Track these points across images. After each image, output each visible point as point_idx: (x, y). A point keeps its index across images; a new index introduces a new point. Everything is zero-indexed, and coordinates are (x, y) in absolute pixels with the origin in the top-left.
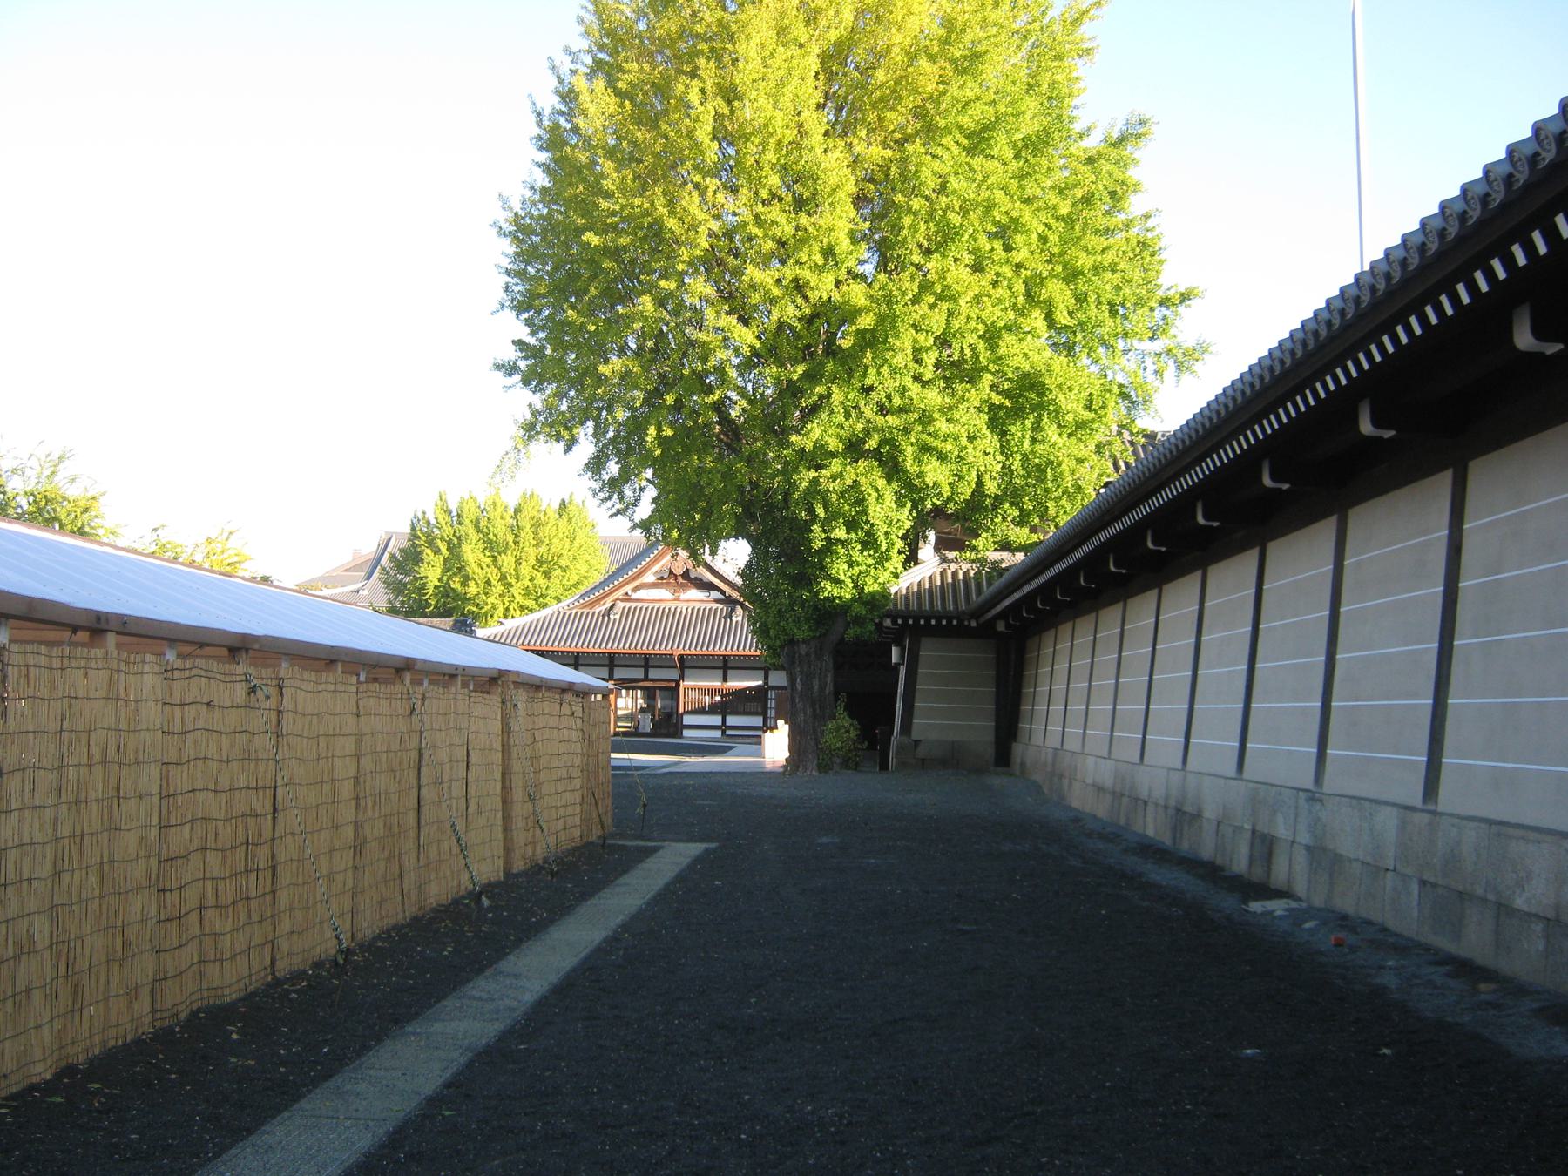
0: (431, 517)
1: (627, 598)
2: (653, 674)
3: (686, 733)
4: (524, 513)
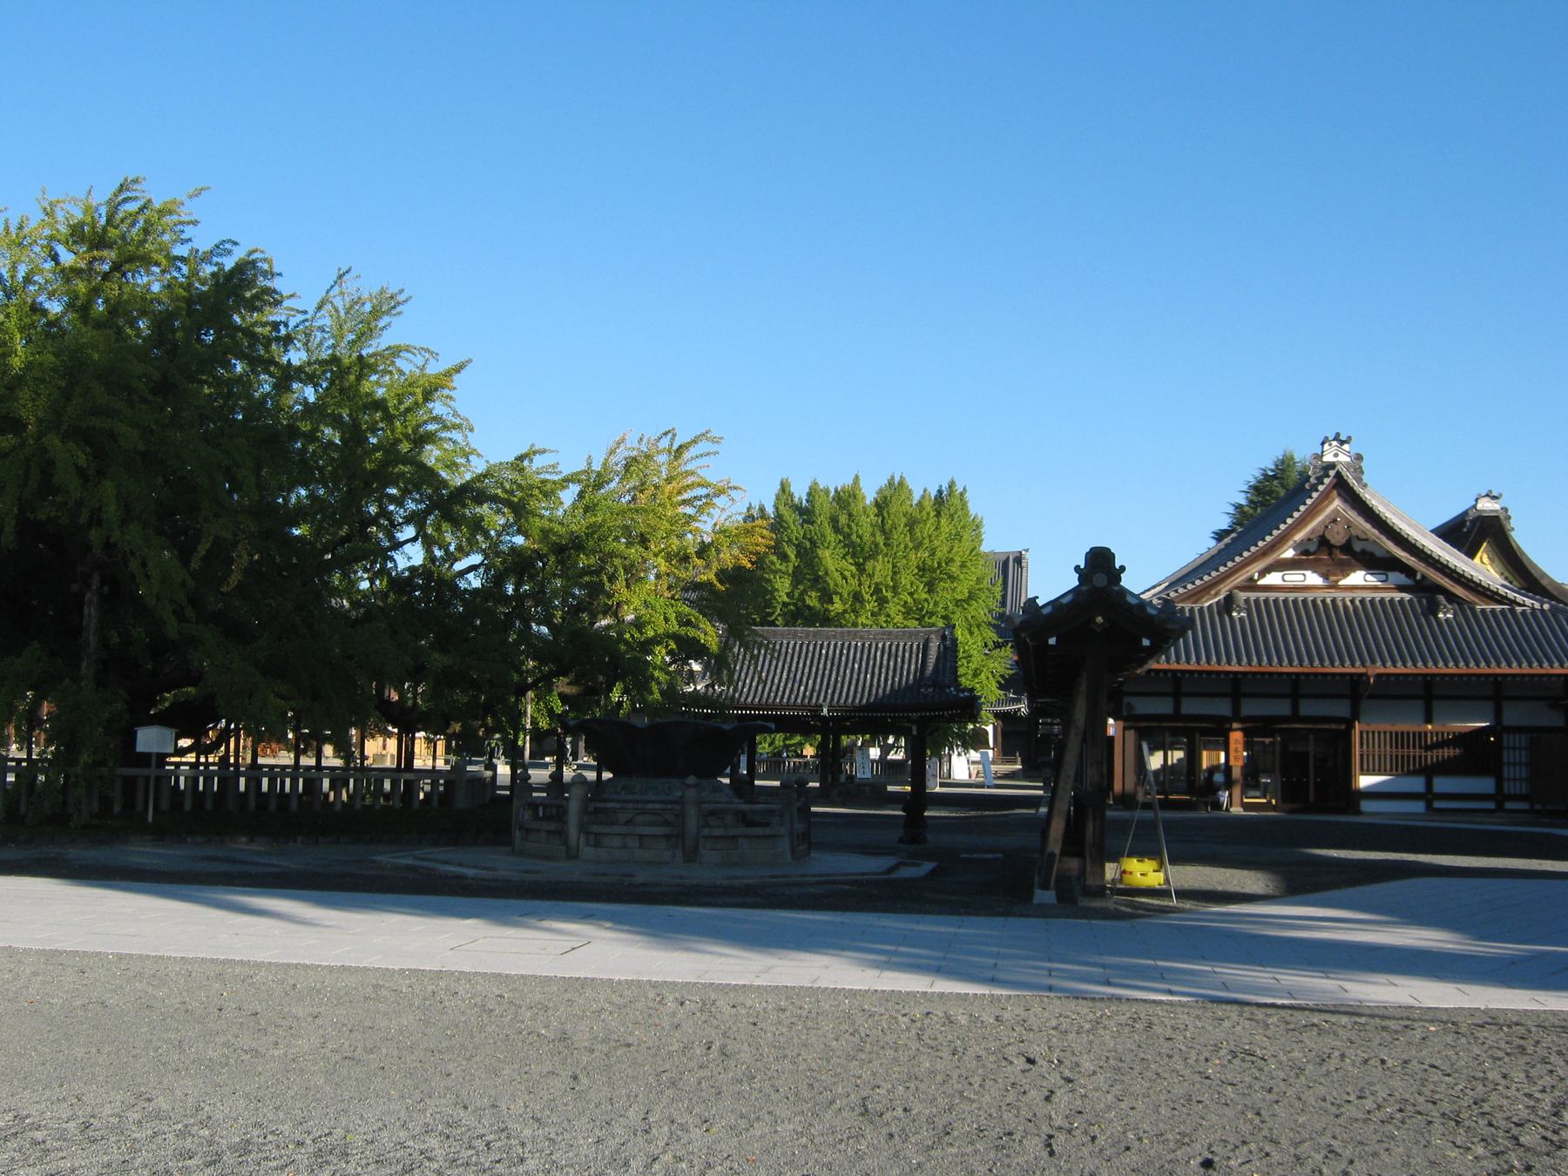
0: (770, 510)
1: (1250, 585)
2: (1308, 708)
3: (1366, 806)
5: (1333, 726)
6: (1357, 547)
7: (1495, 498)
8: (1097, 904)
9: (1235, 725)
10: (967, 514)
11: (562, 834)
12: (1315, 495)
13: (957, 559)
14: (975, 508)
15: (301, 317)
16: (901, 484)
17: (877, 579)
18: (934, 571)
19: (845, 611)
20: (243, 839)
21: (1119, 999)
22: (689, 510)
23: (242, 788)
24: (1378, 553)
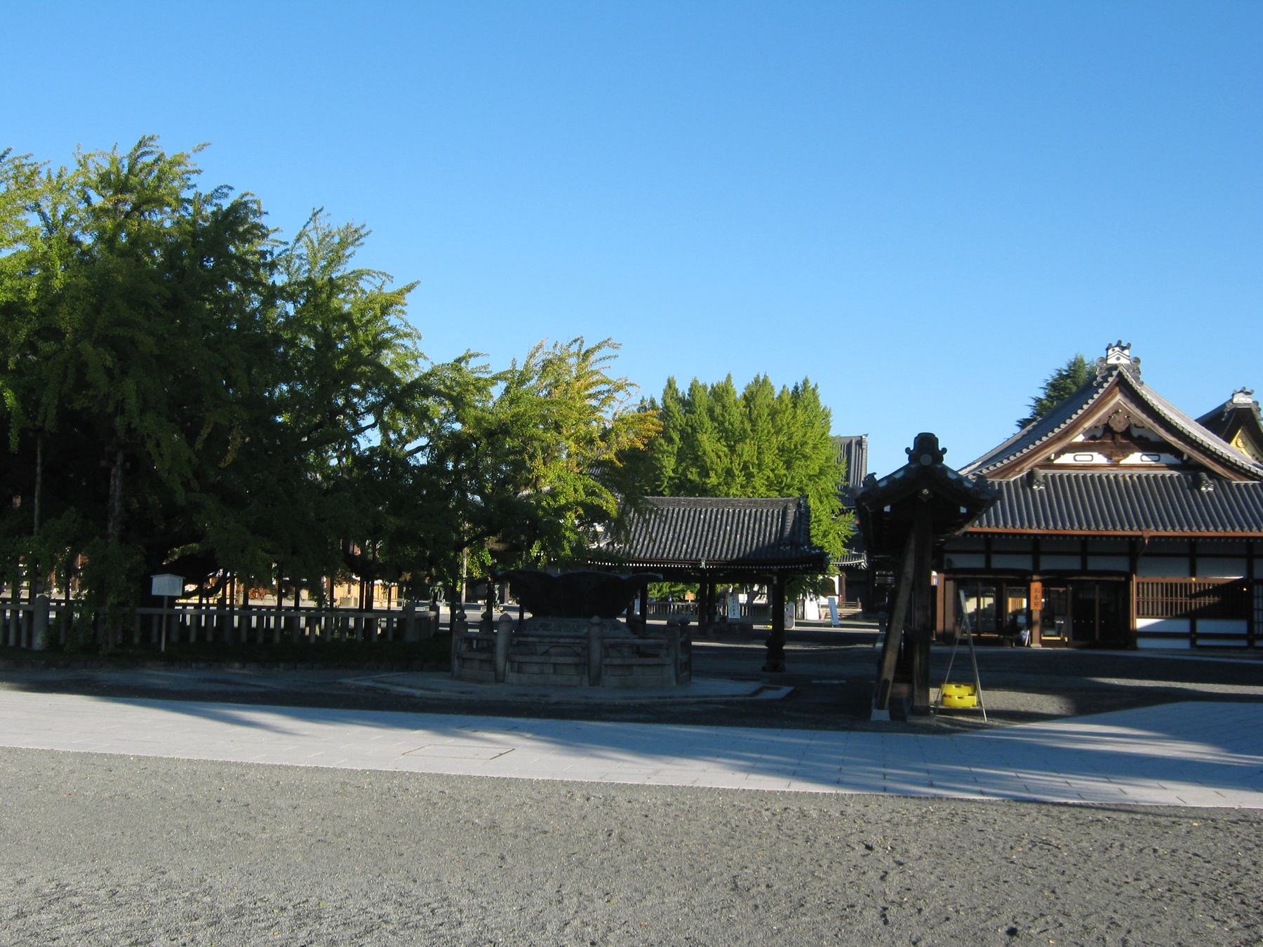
0: (659, 403)
1: (1048, 464)
2: (1095, 564)
3: (1142, 643)
4: (759, 400)
5: (1115, 578)
6: (1135, 433)
7: (1248, 393)
8: (923, 721)
9: (1035, 577)
10: (818, 406)
11: (491, 662)
12: (1101, 391)
13: (810, 442)
14: (823, 402)
15: (283, 247)
16: (765, 381)
17: (745, 458)
18: (790, 451)
19: (719, 484)
20: (237, 665)
21: (940, 798)
22: (594, 403)
23: (236, 624)
24: (1152, 438)
